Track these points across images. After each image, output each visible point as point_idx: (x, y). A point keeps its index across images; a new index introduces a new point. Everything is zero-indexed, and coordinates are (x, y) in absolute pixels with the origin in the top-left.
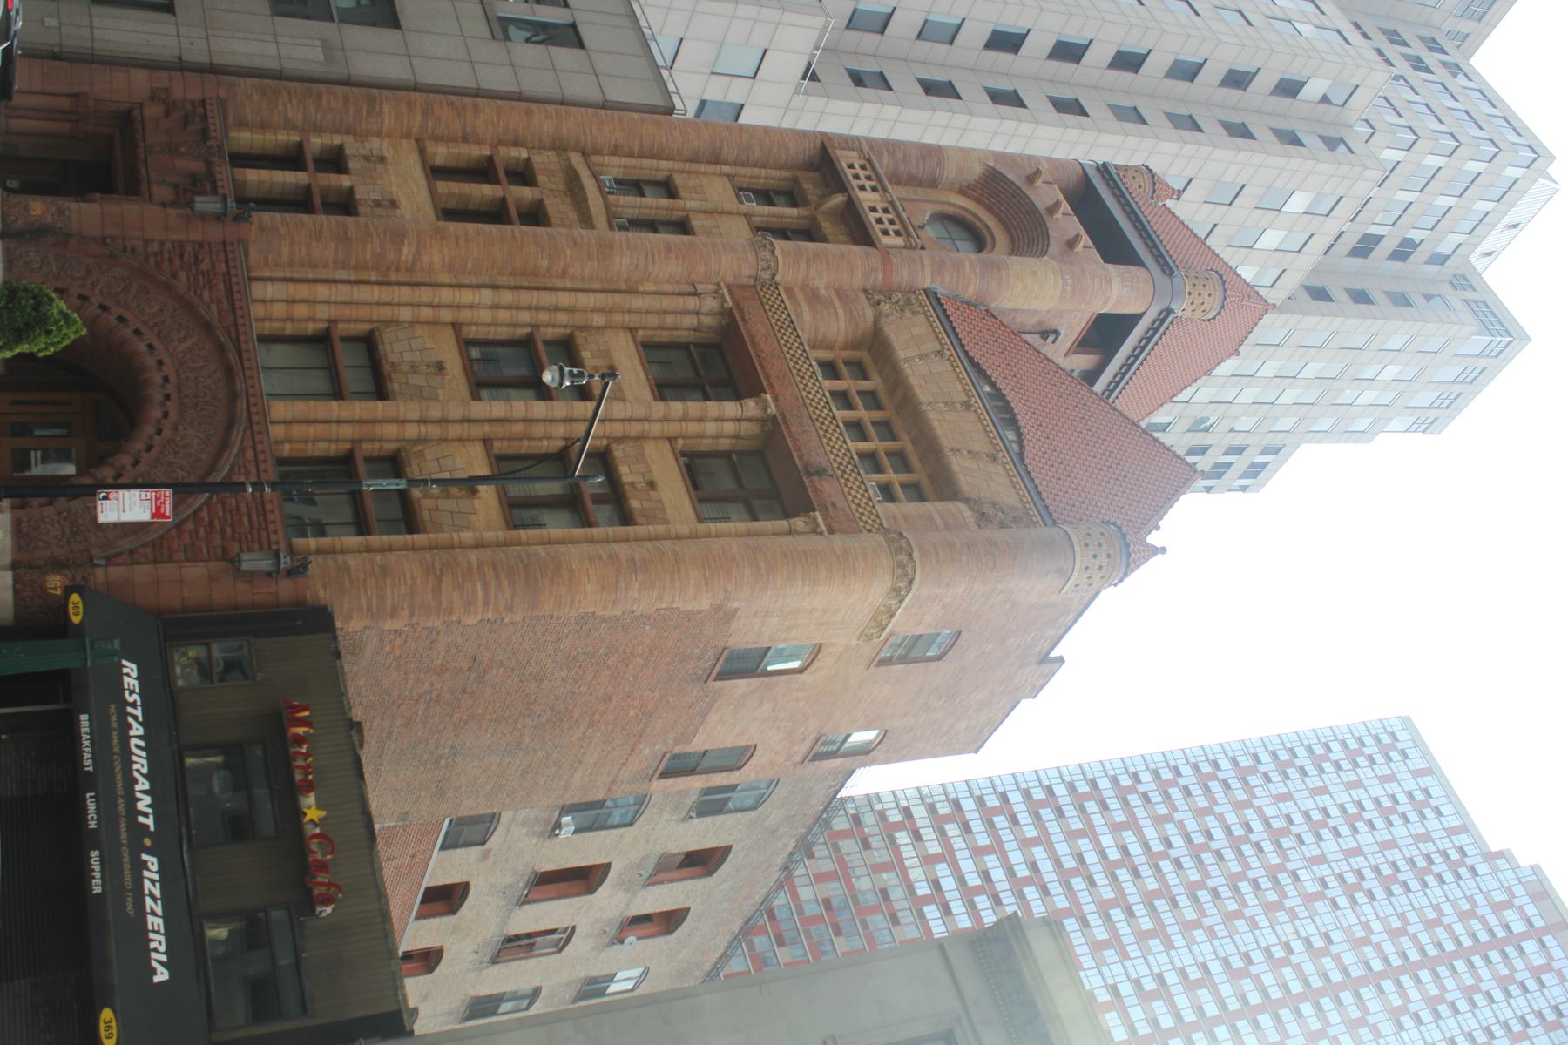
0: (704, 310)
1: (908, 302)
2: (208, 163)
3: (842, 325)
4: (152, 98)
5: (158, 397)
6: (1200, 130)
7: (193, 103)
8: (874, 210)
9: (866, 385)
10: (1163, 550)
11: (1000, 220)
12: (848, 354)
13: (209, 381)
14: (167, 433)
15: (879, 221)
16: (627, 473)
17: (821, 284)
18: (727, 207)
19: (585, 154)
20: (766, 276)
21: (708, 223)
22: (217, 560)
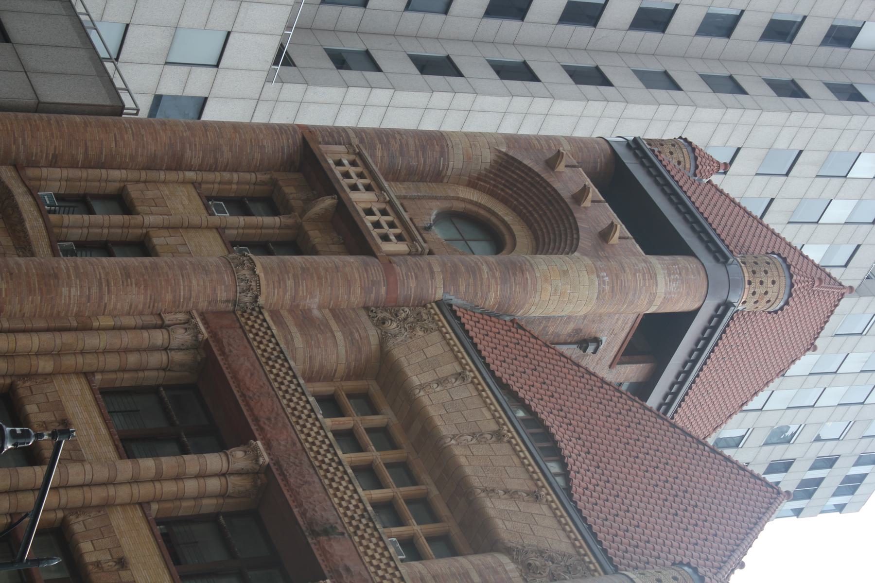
0: (175, 343)
1: (419, 318)
3: (342, 350)
6: (743, 92)
8: (369, 212)
9: (375, 420)
11: (520, 214)
12: (350, 385)
15: (377, 225)
16: (90, 551)
17: (313, 303)
18: (195, 220)
19: (17, 167)
20: (247, 299)
21: (171, 241)
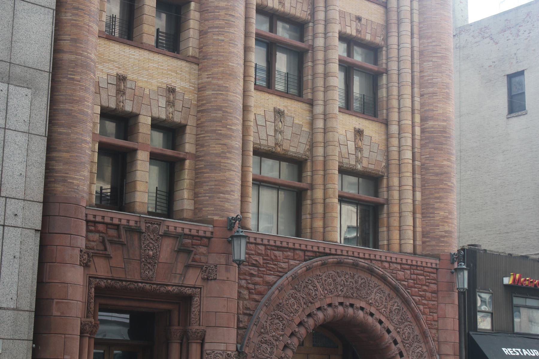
2: (166, 235)
4: (86, 266)
7: (88, 231)
13: (343, 278)
14: (373, 310)
22: (437, 297)
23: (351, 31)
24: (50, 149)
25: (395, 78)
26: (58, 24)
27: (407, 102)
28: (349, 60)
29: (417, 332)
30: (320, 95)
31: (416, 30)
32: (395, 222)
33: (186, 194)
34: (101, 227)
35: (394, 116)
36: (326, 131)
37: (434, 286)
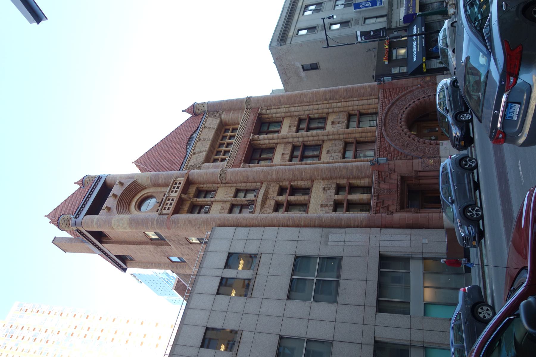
2: (379, 186)
4: (392, 213)
5: (403, 120)
7: (379, 213)
8: (176, 191)
10: (183, 111)
23: (294, 129)
24: (350, 227)
25: (311, 112)
26: (305, 226)
27: (320, 106)
28: (305, 129)
29: (410, 94)
30: (320, 138)
31: (292, 106)
32: (366, 107)
33: (362, 181)
34: (378, 209)
35: (325, 111)
36: (333, 135)
37: (391, 90)
